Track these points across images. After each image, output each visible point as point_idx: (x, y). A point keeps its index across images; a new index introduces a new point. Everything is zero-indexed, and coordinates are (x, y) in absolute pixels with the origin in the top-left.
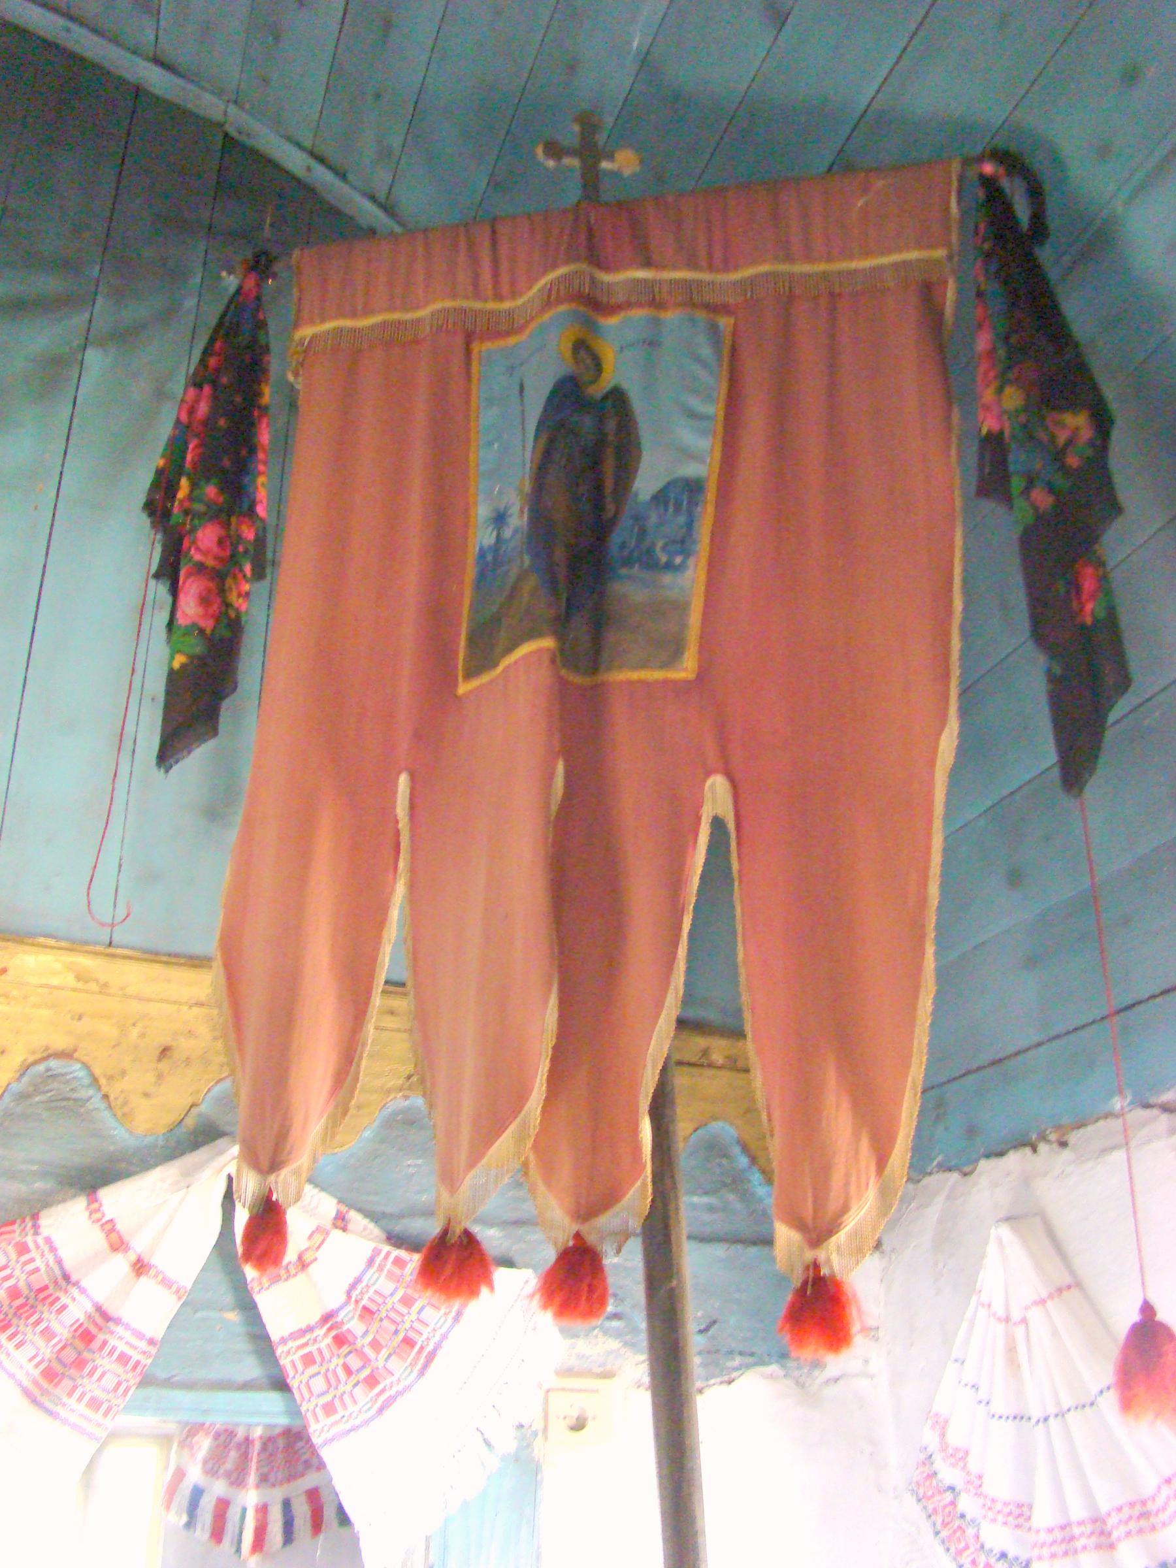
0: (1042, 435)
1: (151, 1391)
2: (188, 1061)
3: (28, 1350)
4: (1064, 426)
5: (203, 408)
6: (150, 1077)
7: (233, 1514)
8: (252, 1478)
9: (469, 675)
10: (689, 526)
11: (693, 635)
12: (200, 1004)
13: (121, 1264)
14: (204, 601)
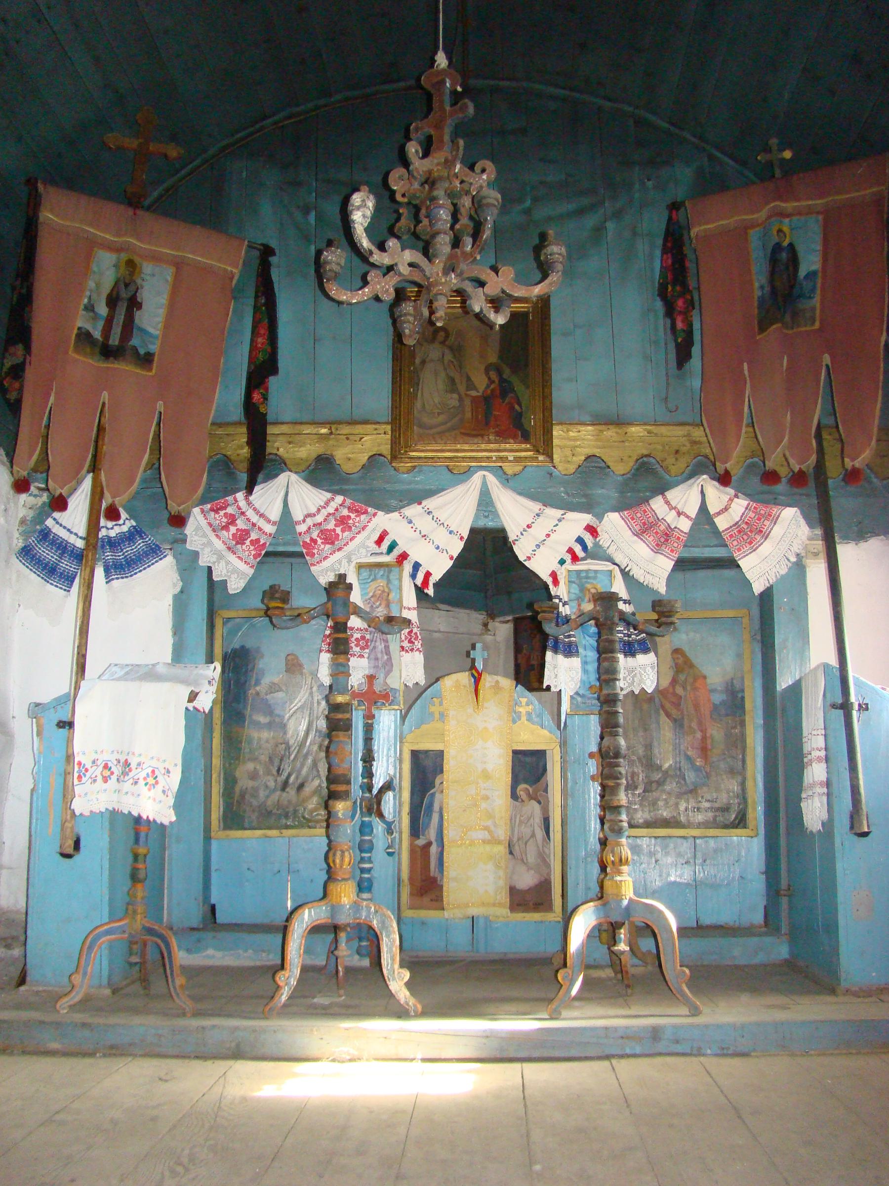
1: (686, 548)
2: (684, 453)
3: (652, 538)
5: (670, 262)
6: (674, 460)
9: (759, 334)
12: (684, 436)
13: (674, 513)
14: (683, 322)
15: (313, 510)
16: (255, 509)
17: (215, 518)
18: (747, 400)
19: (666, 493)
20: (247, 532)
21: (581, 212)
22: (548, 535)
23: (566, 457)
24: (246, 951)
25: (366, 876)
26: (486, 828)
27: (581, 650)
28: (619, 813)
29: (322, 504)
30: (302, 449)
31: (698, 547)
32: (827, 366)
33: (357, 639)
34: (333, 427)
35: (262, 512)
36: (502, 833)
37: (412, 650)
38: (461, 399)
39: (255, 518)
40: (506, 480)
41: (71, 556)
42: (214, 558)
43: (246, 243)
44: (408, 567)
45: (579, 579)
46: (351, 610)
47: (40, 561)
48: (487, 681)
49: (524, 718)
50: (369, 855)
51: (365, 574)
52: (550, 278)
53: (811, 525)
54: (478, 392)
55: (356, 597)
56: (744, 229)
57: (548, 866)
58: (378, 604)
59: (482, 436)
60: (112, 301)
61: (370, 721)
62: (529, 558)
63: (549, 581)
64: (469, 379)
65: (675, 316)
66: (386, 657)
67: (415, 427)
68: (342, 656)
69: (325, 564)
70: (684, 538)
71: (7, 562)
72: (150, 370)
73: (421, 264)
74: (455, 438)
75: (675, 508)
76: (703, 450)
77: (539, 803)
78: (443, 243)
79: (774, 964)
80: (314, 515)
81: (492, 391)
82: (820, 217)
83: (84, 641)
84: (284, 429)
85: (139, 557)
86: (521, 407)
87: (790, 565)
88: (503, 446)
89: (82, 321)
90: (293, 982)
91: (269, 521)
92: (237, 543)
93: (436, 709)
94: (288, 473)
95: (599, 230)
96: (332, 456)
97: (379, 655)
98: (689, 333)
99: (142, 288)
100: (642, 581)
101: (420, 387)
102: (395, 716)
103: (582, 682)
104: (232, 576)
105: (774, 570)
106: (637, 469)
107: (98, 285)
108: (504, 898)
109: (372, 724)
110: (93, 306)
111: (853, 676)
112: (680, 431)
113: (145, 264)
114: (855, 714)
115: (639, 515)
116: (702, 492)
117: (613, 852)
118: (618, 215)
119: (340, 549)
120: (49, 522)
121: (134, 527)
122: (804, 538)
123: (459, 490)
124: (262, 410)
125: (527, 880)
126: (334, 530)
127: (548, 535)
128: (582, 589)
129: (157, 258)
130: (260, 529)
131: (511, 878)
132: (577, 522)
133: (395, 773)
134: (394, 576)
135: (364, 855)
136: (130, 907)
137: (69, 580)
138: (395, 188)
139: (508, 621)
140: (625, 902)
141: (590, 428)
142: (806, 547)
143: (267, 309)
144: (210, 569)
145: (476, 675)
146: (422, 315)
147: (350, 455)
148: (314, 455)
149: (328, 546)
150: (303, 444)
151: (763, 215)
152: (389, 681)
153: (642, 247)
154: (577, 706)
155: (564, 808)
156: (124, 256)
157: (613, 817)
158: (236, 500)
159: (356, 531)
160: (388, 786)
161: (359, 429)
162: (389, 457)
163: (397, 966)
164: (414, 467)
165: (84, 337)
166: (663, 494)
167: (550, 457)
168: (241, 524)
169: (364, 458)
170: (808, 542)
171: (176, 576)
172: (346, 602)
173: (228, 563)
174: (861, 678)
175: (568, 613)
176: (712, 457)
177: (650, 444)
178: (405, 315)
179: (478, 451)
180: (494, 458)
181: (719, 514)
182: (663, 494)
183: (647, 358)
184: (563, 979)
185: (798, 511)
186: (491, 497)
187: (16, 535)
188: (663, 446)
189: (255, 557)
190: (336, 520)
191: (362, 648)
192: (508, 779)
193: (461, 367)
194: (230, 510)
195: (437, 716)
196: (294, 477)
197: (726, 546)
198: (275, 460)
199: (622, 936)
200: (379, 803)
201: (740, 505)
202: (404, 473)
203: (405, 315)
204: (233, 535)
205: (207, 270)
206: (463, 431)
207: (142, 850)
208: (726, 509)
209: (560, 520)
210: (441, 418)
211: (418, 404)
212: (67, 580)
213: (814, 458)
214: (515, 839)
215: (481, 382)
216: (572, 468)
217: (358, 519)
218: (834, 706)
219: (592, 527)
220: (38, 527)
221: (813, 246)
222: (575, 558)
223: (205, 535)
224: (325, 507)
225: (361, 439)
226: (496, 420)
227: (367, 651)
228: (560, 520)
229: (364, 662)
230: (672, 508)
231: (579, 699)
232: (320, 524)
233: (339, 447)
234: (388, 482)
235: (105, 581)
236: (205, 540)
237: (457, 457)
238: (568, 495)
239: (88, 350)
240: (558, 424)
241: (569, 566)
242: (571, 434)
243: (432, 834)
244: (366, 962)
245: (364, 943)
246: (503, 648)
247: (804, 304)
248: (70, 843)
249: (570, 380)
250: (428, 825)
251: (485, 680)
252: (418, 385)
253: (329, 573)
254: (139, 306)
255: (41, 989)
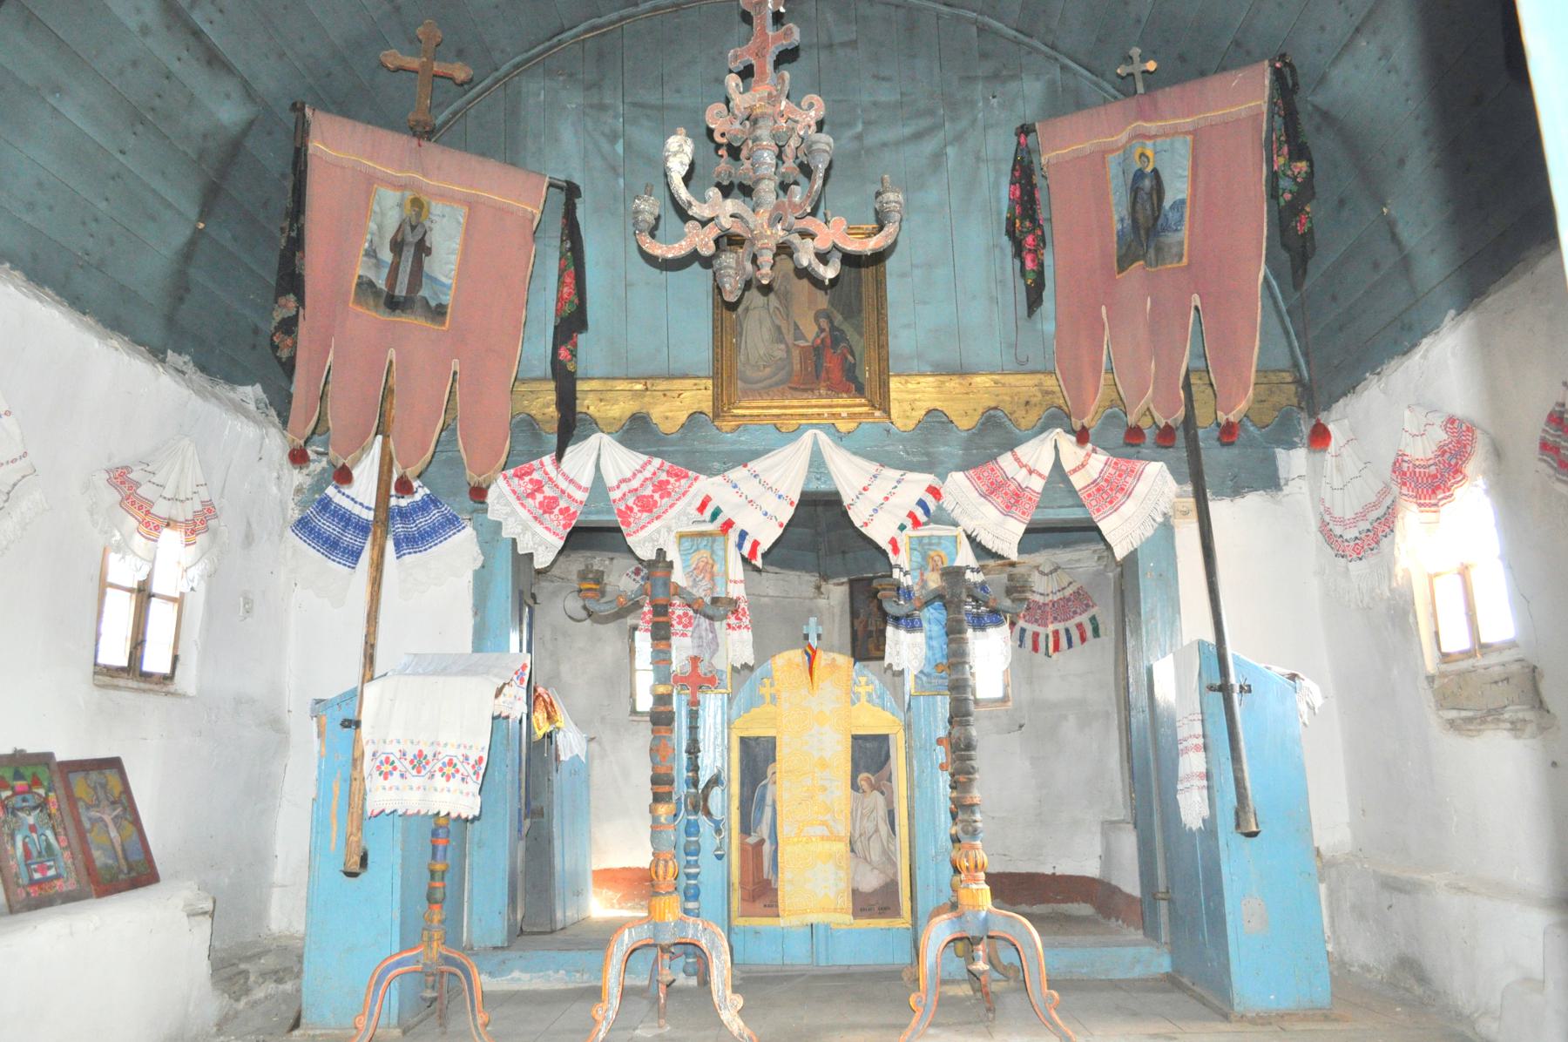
0: (1289, 173)
2: (1035, 405)
4: (1296, 167)
5: (1018, 193)
6: (1024, 412)
7: (1042, 639)
8: (1050, 619)
10: (1182, 216)
11: (1185, 252)
13: (1024, 471)
14: (1033, 261)
15: (628, 474)
16: (564, 474)
17: (520, 485)
18: (1105, 347)
19: (1016, 450)
20: (555, 500)
21: (918, 136)
22: (887, 499)
23: (904, 411)
24: (557, 971)
25: (693, 882)
26: (824, 823)
27: (925, 625)
28: (973, 813)
29: (638, 467)
30: (615, 407)
31: (1052, 508)
32: (1197, 308)
33: (679, 617)
34: (649, 382)
35: (571, 477)
36: (843, 829)
37: (739, 627)
38: (788, 351)
39: (563, 484)
40: (839, 438)
41: (355, 528)
42: (519, 529)
43: (547, 179)
44: (733, 536)
45: (921, 545)
46: (672, 591)
47: (319, 534)
48: (823, 658)
49: (864, 698)
50: (695, 858)
51: (687, 544)
52: (886, 229)
53: (1179, 482)
54: (807, 341)
55: (679, 577)
56: (1104, 153)
57: (894, 864)
58: (701, 577)
59: (812, 390)
60: (397, 246)
61: (694, 708)
62: (866, 524)
63: (889, 549)
64: (797, 327)
65: (1024, 253)
66: (711, 635)
67: (739, 382)
68: (664, 642)
69: (643, 534)
70: (1036, 498)
71: (281, 536)
72: (443, 323)
73: (745, 215)
74: (783, 394)
75: (1026, 466)
76: (1056, 400)
77: (882, 793)
78: (767, 190)
79: (1155, 980)
80: (630, 480)
81: (823, 340)
82: (1189, 138)
83: (372, 629)
84: (594, 385)
85: (434, 529)
86: (853, 356)
87: (1156, 525)
88: (836, 401)
89: (362, 269)
90: (612, 1015)
91: (579, 487)
92: (545, 512)
93: (766, 691)
94: (599, 434)
95: (938, 158)
96: (648, 414)
97: (704, 634)
98: (1040, 274)
99: (431, 230)
100: (990, 547)
101: (744, 338)
102: (722, 700)
103: (927, 659)
104: (540, 548)
105: (1138, 532)
106: (983, 424)
107: (380, 227)
108: (846, 902)
109: (697, 711)
110: (375, 251)
111: (1233, 655)
112: (1029, 380)
113: (433, 204)
114: (1236, 697)
115: (986, 474)
116: (1056, 447)
117: (967, 856)
118: (959, 138)
119: (658, 517)
120: (331, 491)
121: (428, 496)
122: (1172, 495)
123: (789, 450)
124: (570, 367)
125: (871, 881)
126: (652, 497)
127: (887, 499)
128: (925, 557)
129: (443, 196)
130: (570, 496)
131: (853, 878)
132: (918, 484)
133: (723, 766)
134: (718, 546)
135: (689, 858)
136: (426, 932)
137: (354, 555)
138: (713, 126)
139: (842, 584)
140: (983, 914)
141: (931, 379)
142: (1173, 507)
143: (573, 254)
144: (514, 541)
145: (810, 652)
146: (744, 268)
147: (668, 414)
148: (628, 414)
149: (645, 514)
150: (616, 402)
151: (1122, 137)
152: (714, 661)
153: (986, 174)
154: (923, 686)
155: (910, 798)
156: (409, 195)
157: (966, 817)
158: (542, 464)
159: (676, 497)
160: (715, 781)
161: (677, 384)
162: (711, 415)
163: (729, 992)
164: (739, 426)
165: (366, 286)
166: (1012, 450)
167: (887, 411)
168: (548, 491)
169: (683, 417)
170: (1176, 500)
171: (477, 549)
172: (667, 582)
173: (534, 534)
174: (1242, 657)
175: (910, 584)
176: (1065, 408)
177: (997, 395)
178: (726, 267)
179: (808, 407)
180: (826, 415)
181: (1075, 471)
182: (1012, 450)
183: (993, 300)
184: (917, 1003)
185: (1165, 467)
186: (823, 458)
187: (292, 505)
188: (1012, 397)
189: (565, 527)
190: (654, 485)
191: (685, 626)
192: (847, 767)
193: (788, 315)
194: (536, 476)
195: (768, 699)
196: (606, 439)
197: (1084, 506)
198: (585, 420)
199: (981, 953)
200: (706, 799)
201: (1098, 462)
202: (727, 433)
203: (726, 267)
204: (541, 503)
205: (503, 211)
206: (792, 385)
207: (439, 867)
208: (1083, 465)
209: (899, 482)
210: (768, 370)
211: (742, 358)
212: (352, 555)
213: (1181, 413)
214: (857, 835)
215: (810, 331)
216: (911, 425)
217: (678, 484)
218: (1211, 688)
219: (935, 488)
220: (317, 496)
221: (1180, 171)
222: (916, 523)
223: (508, 504)
224: (641, 472)
225: (680, 395)
226: (827, 373)
227: (690, 629)
228: (899, 482)
229: (687, 641)
230: (1022, 465)
231: (924, 679)
232: (636, 490)
233: (656, 404)
234: (710, 443)
235: (395, 556)
236: (508, 509)
237: (786, 415)
238: (908, 454)
239: (371, 302)
240: (895, 375)
241: (909, 531)
242: (910, 386)
243: (764, 830)
244: (693, 982)
245: (690, 960)
246: (837, 611)
247: (1170, 238)
248: (357, 859)
249: (908, 326)
250: (760, 821)
251: (820, 657)
252: (741, 336)
253: (647, 544)
254: (428, 251)
255: (318, 1032)
